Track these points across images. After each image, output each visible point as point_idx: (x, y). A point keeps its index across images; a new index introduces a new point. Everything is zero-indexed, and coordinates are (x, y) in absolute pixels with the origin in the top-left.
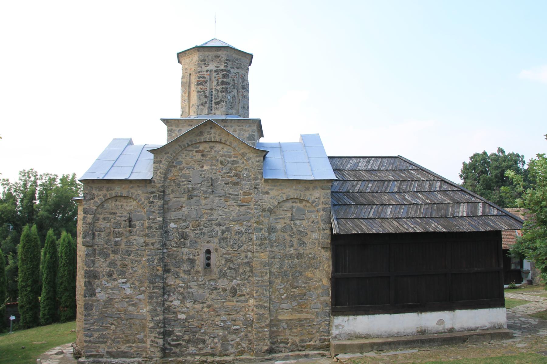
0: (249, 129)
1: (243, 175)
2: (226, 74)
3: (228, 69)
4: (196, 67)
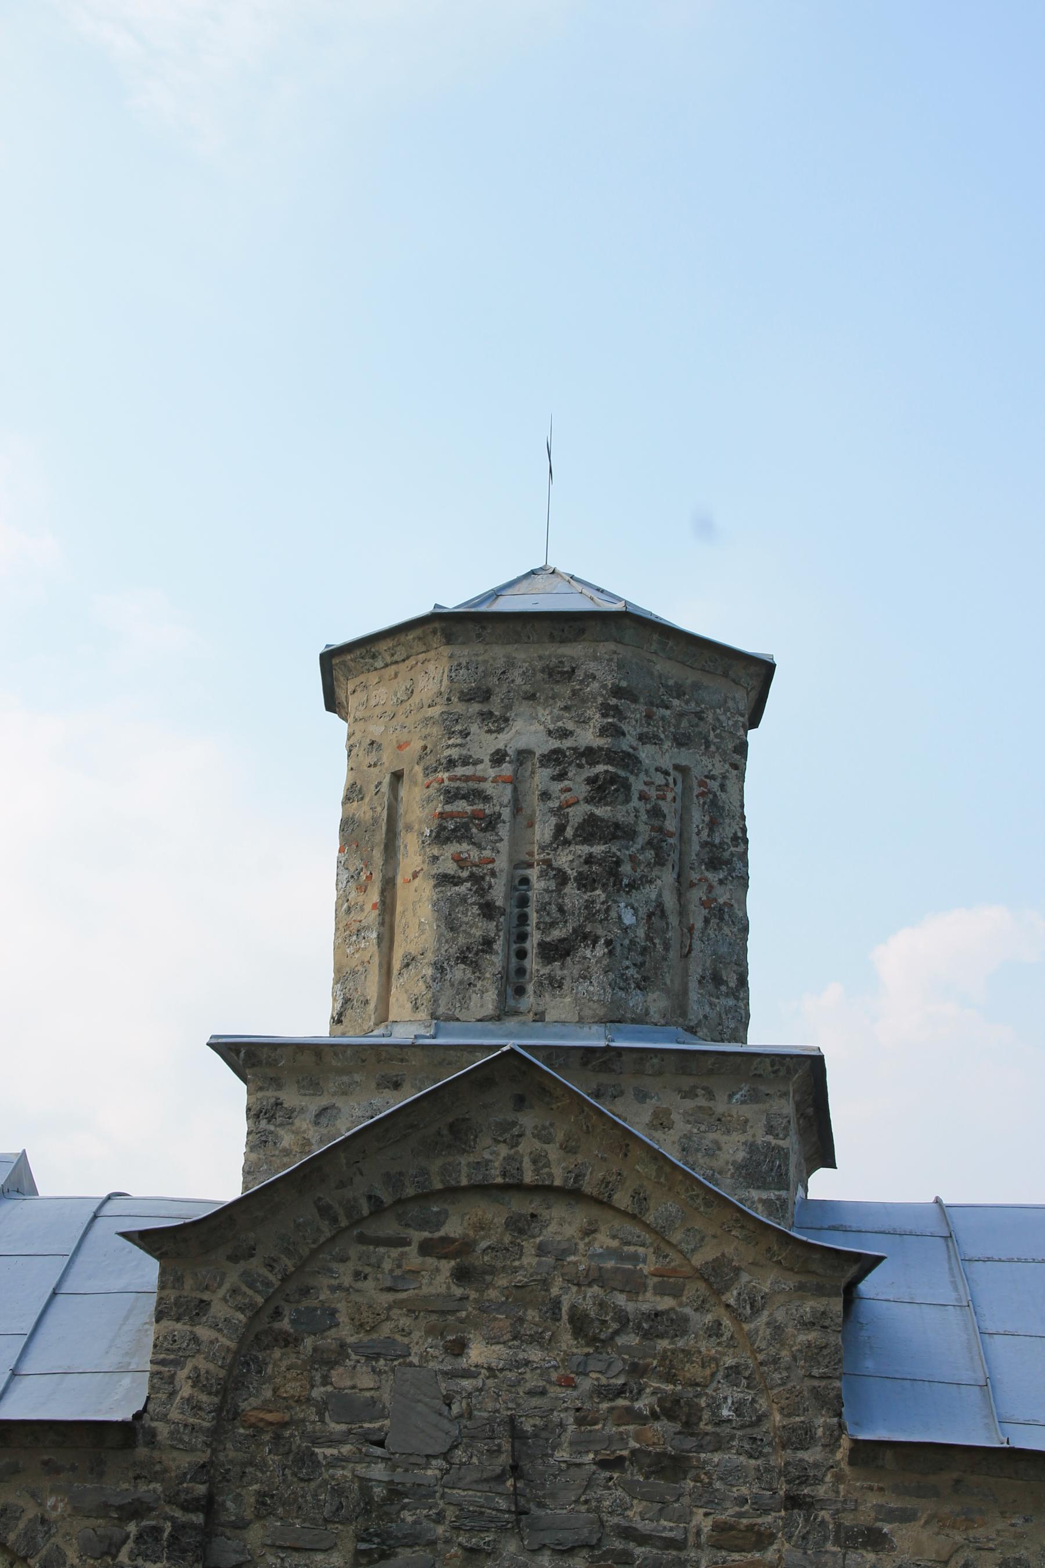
0: (747, 1111)
1: (715, 1407)
2: (613, 779)
3: (625, 744)
4: (436, 731)
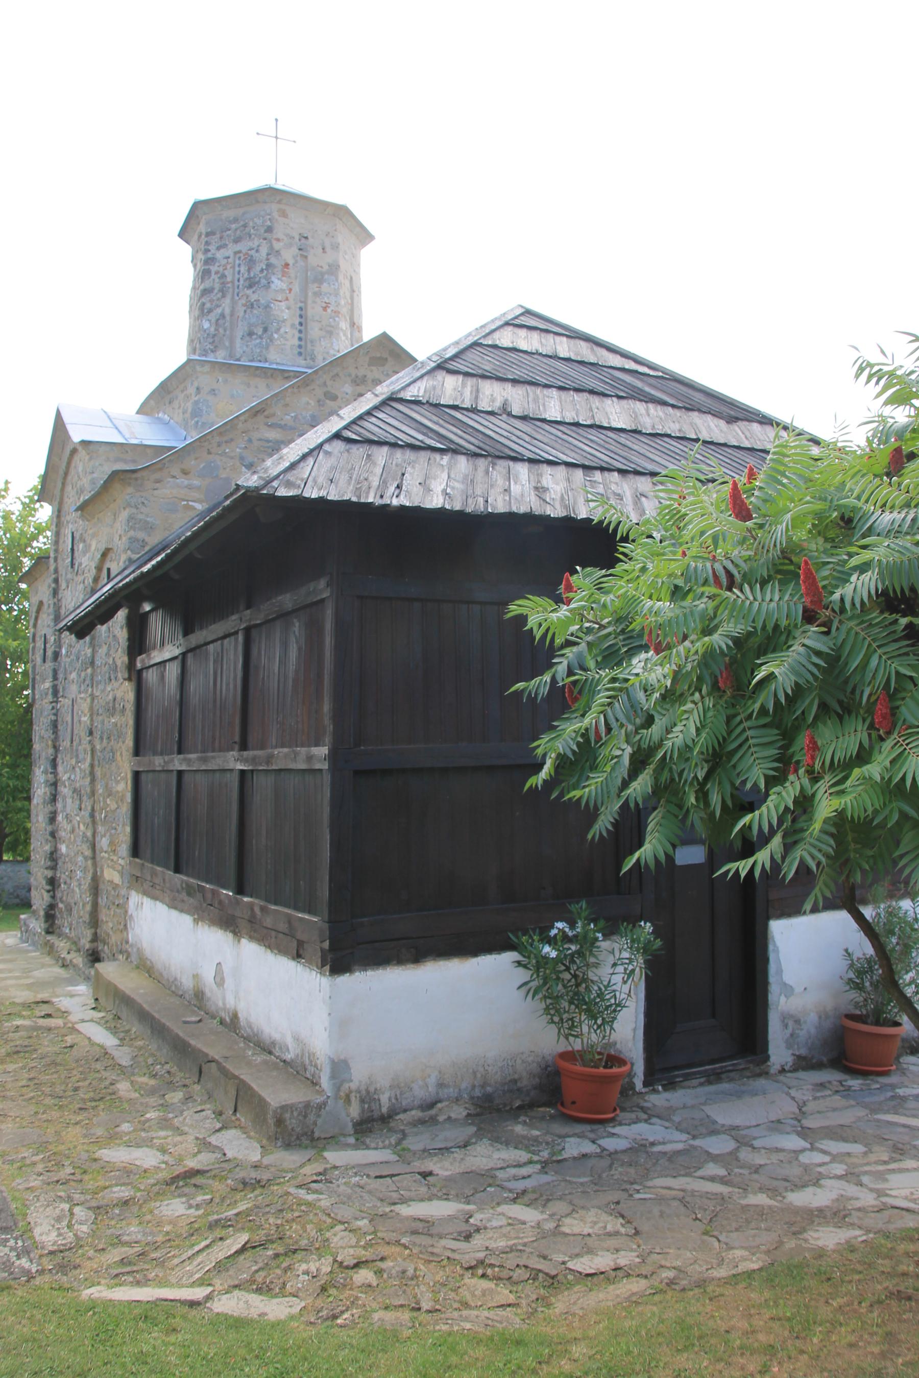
3: (210, 255)
